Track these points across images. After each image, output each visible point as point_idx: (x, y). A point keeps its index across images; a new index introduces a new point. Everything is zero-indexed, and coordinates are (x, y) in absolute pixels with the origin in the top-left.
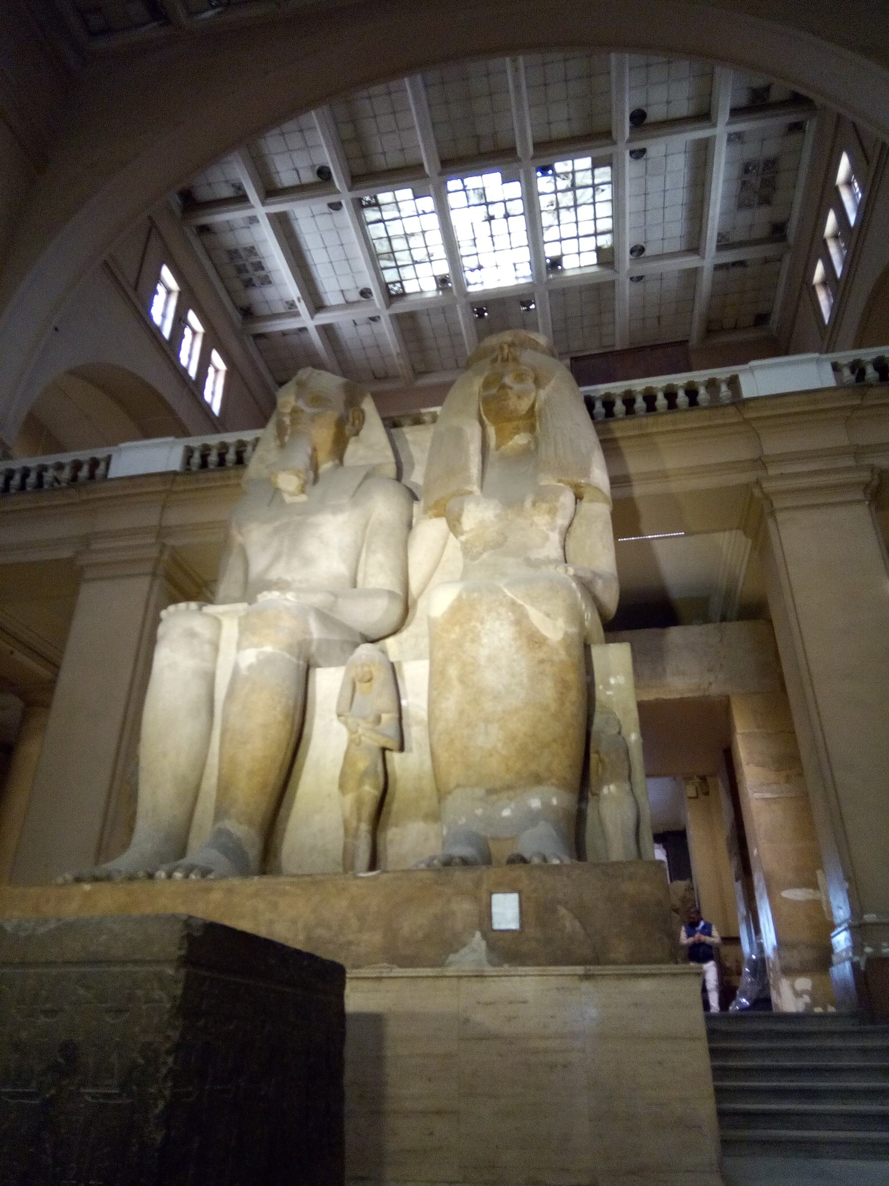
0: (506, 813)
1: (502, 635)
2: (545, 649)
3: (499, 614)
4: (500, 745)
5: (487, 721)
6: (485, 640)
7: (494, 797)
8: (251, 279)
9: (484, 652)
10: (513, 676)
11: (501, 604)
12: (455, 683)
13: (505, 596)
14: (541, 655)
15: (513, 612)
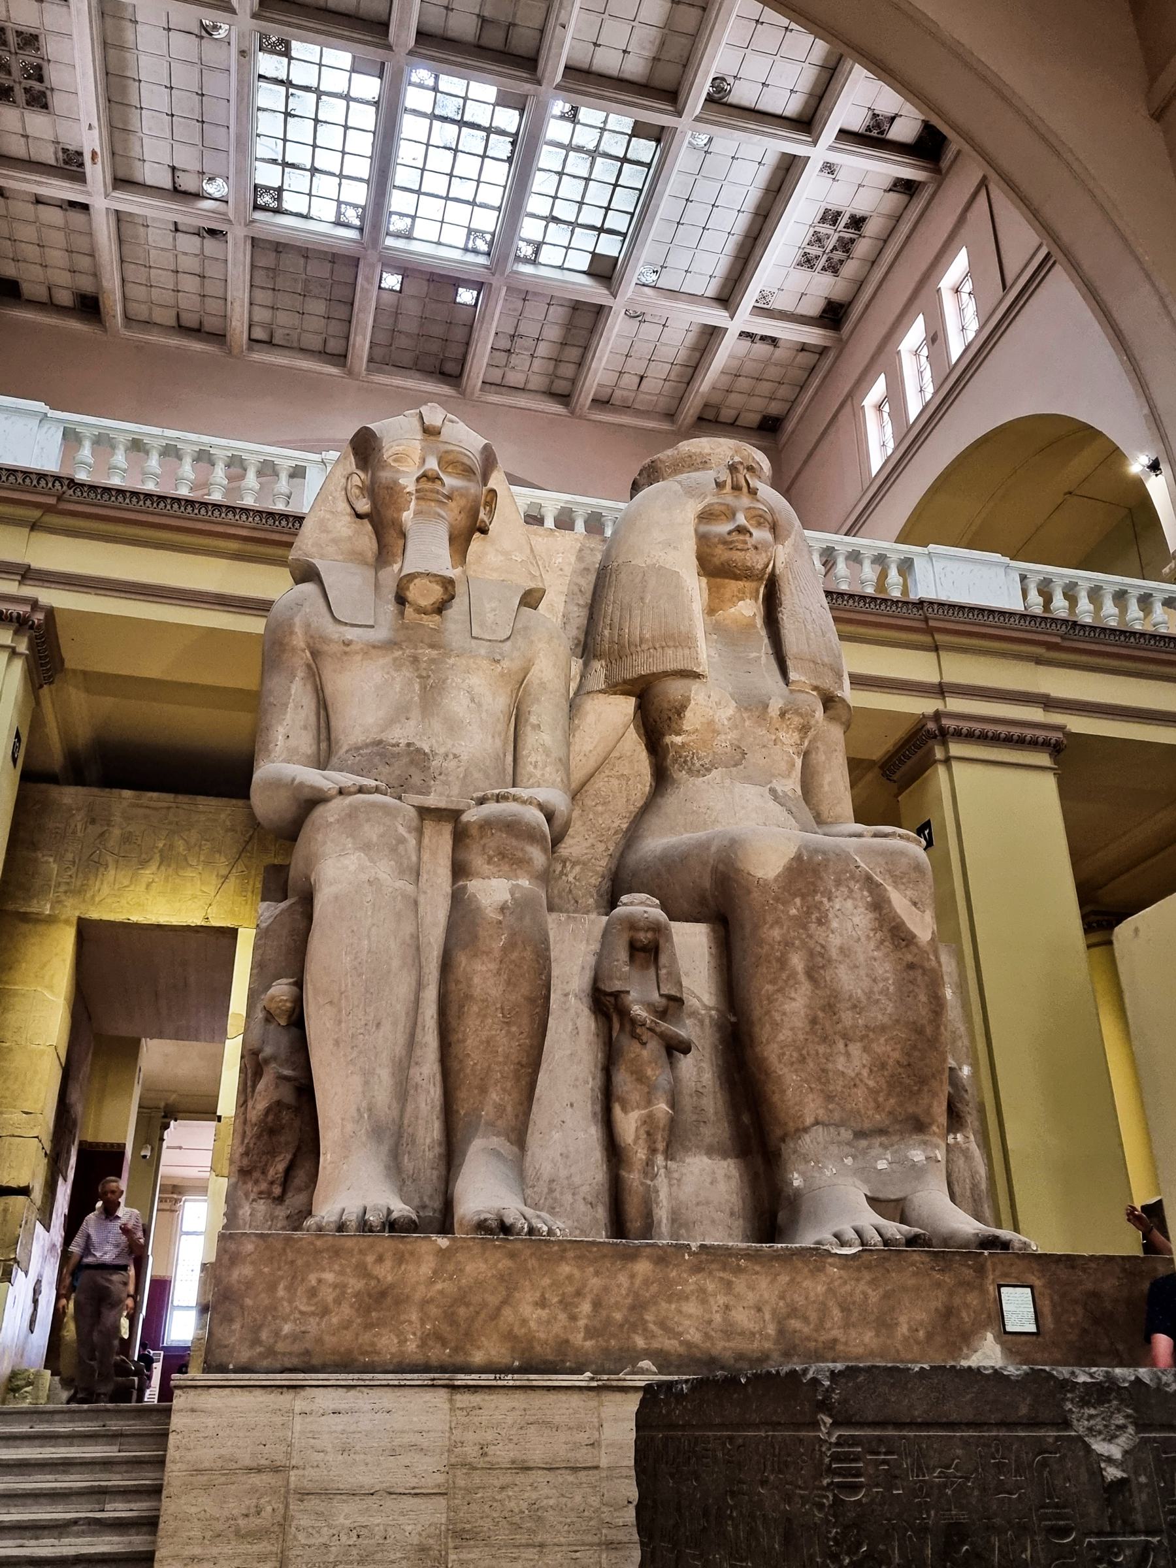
0: (882, 1165)
1: (856, 920)
2: (914, 949)
3: (851, 891)
4: (865, 1072)
5: (847, 1038)
6: (835, 924)
7: (863, 1143)
8: (11, 89)
9: (835, 941)
10: (874, 980)
11: (852, 877)
12: (802, 977)
13: (857, 867)
14: (909, 958)
15: (871, 893)
